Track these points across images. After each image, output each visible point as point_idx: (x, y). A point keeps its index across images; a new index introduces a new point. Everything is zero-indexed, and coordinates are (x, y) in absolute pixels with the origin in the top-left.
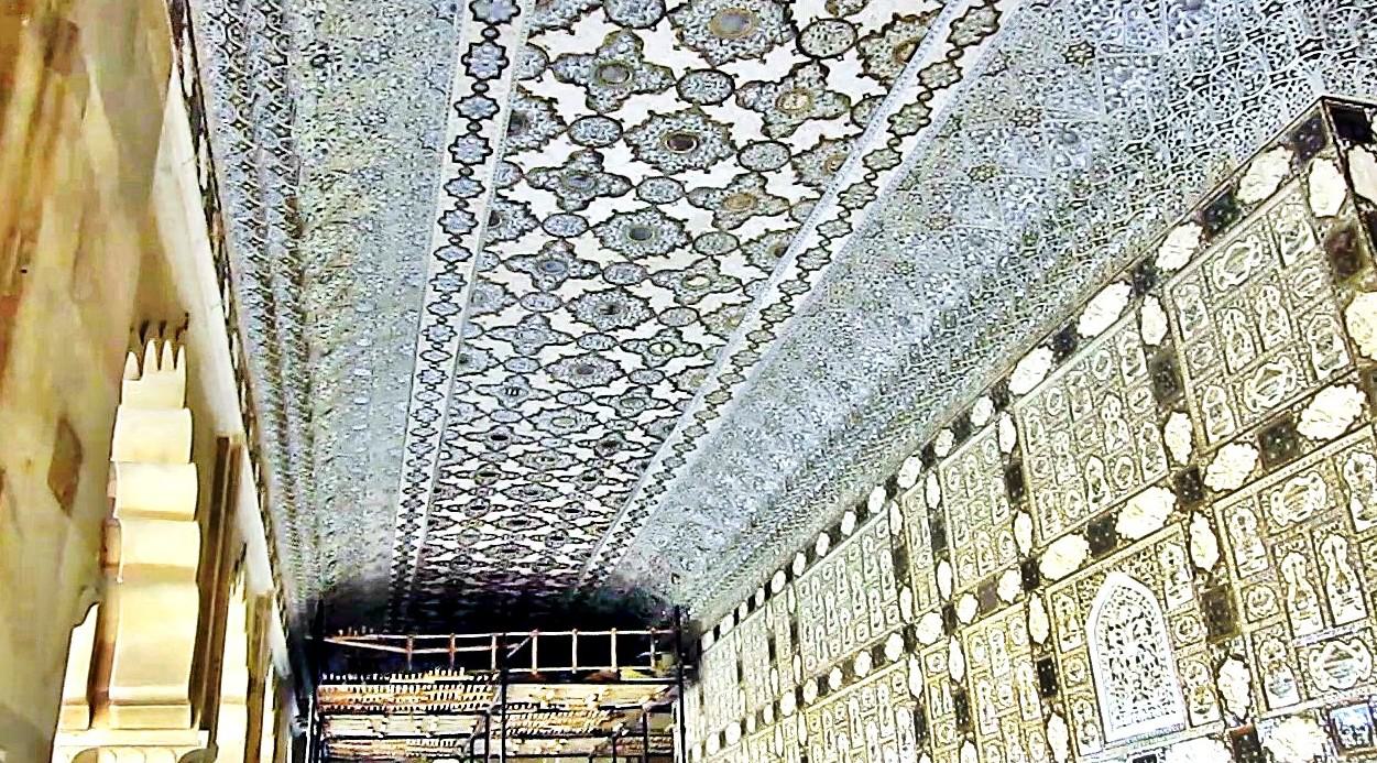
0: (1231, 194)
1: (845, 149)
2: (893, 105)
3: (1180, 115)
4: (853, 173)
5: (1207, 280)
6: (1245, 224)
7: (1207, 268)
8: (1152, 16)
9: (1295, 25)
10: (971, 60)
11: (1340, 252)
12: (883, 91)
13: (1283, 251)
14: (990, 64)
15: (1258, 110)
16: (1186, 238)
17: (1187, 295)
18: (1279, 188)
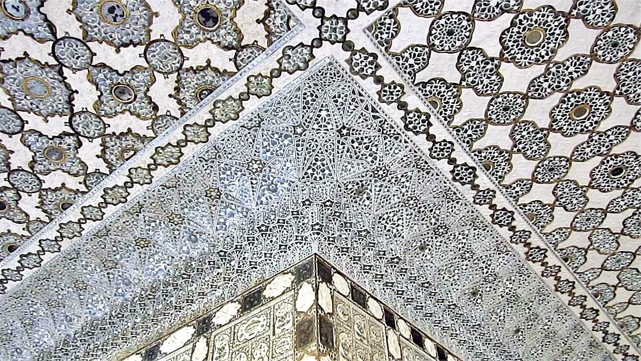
0: (260, 292)
1: (75, 198)
2: (109, 183)
3: (249, 244)
4: (73, 214)
5: (234, 333)
6: (262, 308)
7: (237, 327)
8: (253, 187)
9: (314, 215)
10: (160, 174)
11: (303, 332)
12: (107, 171)
13: (276, 326)
14: (169, 181)
15: (285, 252)
16: (232, 309)
17: (221, 340)
18: (283, 293)
